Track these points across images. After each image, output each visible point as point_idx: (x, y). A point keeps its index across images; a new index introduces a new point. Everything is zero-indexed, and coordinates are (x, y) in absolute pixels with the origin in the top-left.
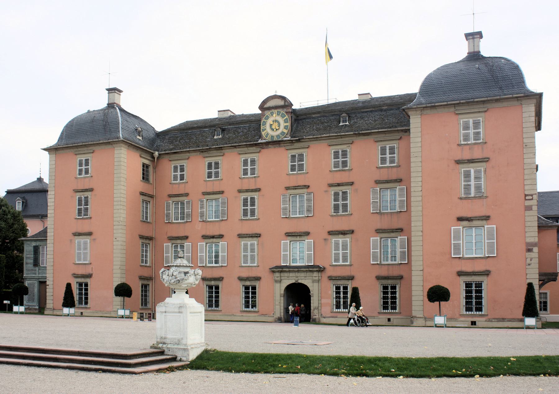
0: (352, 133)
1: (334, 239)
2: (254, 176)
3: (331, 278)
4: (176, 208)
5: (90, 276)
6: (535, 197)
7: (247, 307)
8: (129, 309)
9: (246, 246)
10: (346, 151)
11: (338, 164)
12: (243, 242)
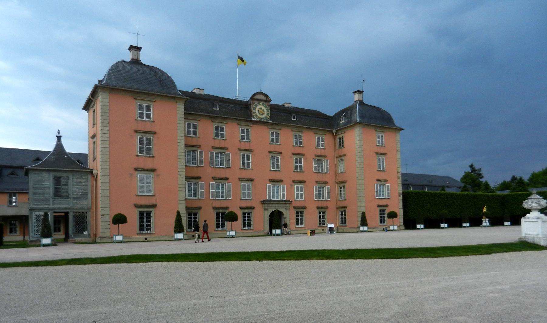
0: (306, 127)
2: (249, 141)
3: (295, 208)
5: (154, 206)
6: (401, 173)
7: (298, 224)
8: (397, 225)
9: (244, 186)
10: (301, 136)
11: (297, 142)
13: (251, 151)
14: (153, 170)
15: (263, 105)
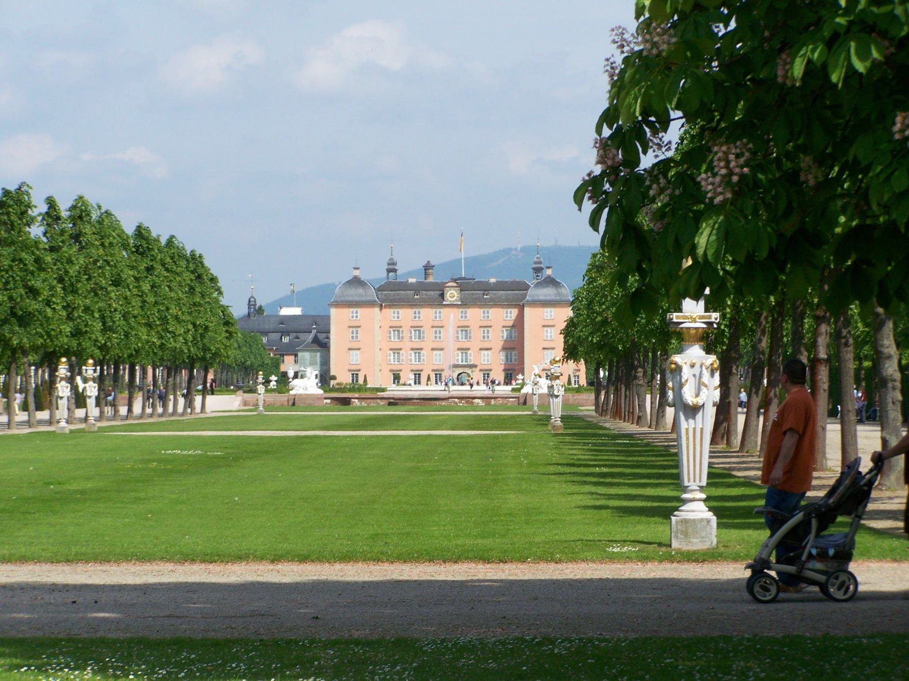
1: (483, 352)
3: (481, 370)
4: (394, 334)
12: (435, 352)
13: (442, 327)
14: (359, 349)
15: (454, 290)
